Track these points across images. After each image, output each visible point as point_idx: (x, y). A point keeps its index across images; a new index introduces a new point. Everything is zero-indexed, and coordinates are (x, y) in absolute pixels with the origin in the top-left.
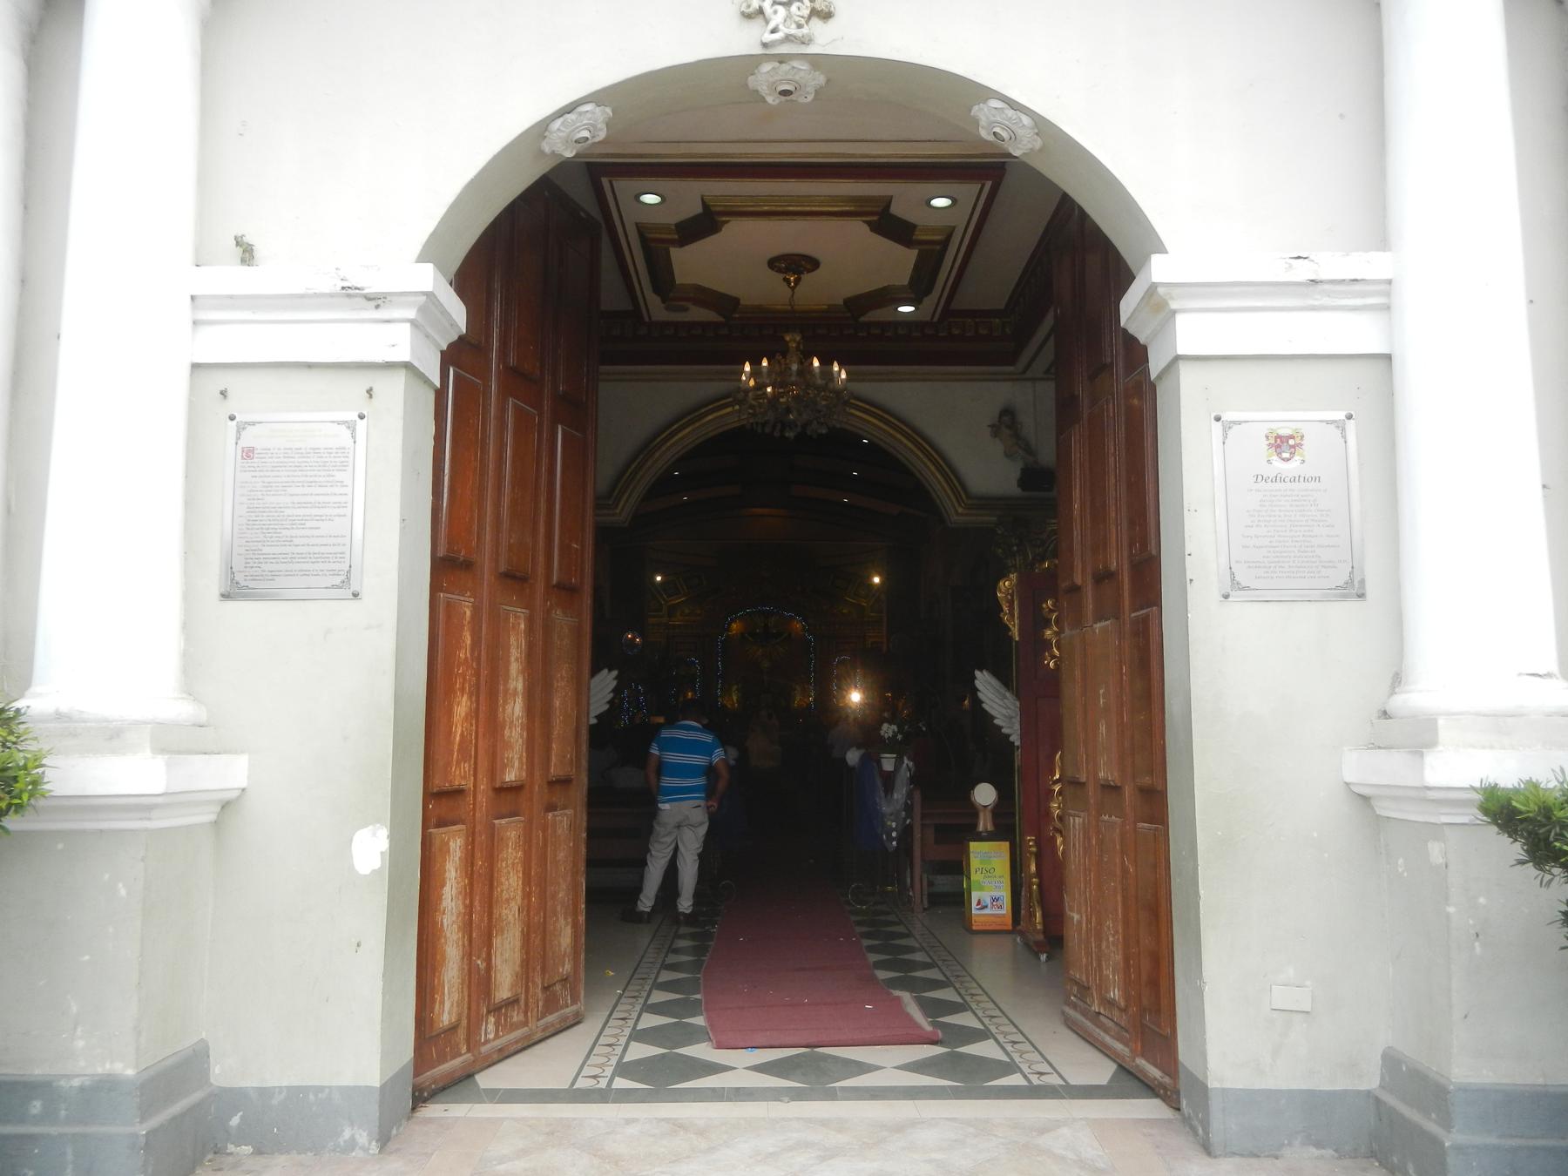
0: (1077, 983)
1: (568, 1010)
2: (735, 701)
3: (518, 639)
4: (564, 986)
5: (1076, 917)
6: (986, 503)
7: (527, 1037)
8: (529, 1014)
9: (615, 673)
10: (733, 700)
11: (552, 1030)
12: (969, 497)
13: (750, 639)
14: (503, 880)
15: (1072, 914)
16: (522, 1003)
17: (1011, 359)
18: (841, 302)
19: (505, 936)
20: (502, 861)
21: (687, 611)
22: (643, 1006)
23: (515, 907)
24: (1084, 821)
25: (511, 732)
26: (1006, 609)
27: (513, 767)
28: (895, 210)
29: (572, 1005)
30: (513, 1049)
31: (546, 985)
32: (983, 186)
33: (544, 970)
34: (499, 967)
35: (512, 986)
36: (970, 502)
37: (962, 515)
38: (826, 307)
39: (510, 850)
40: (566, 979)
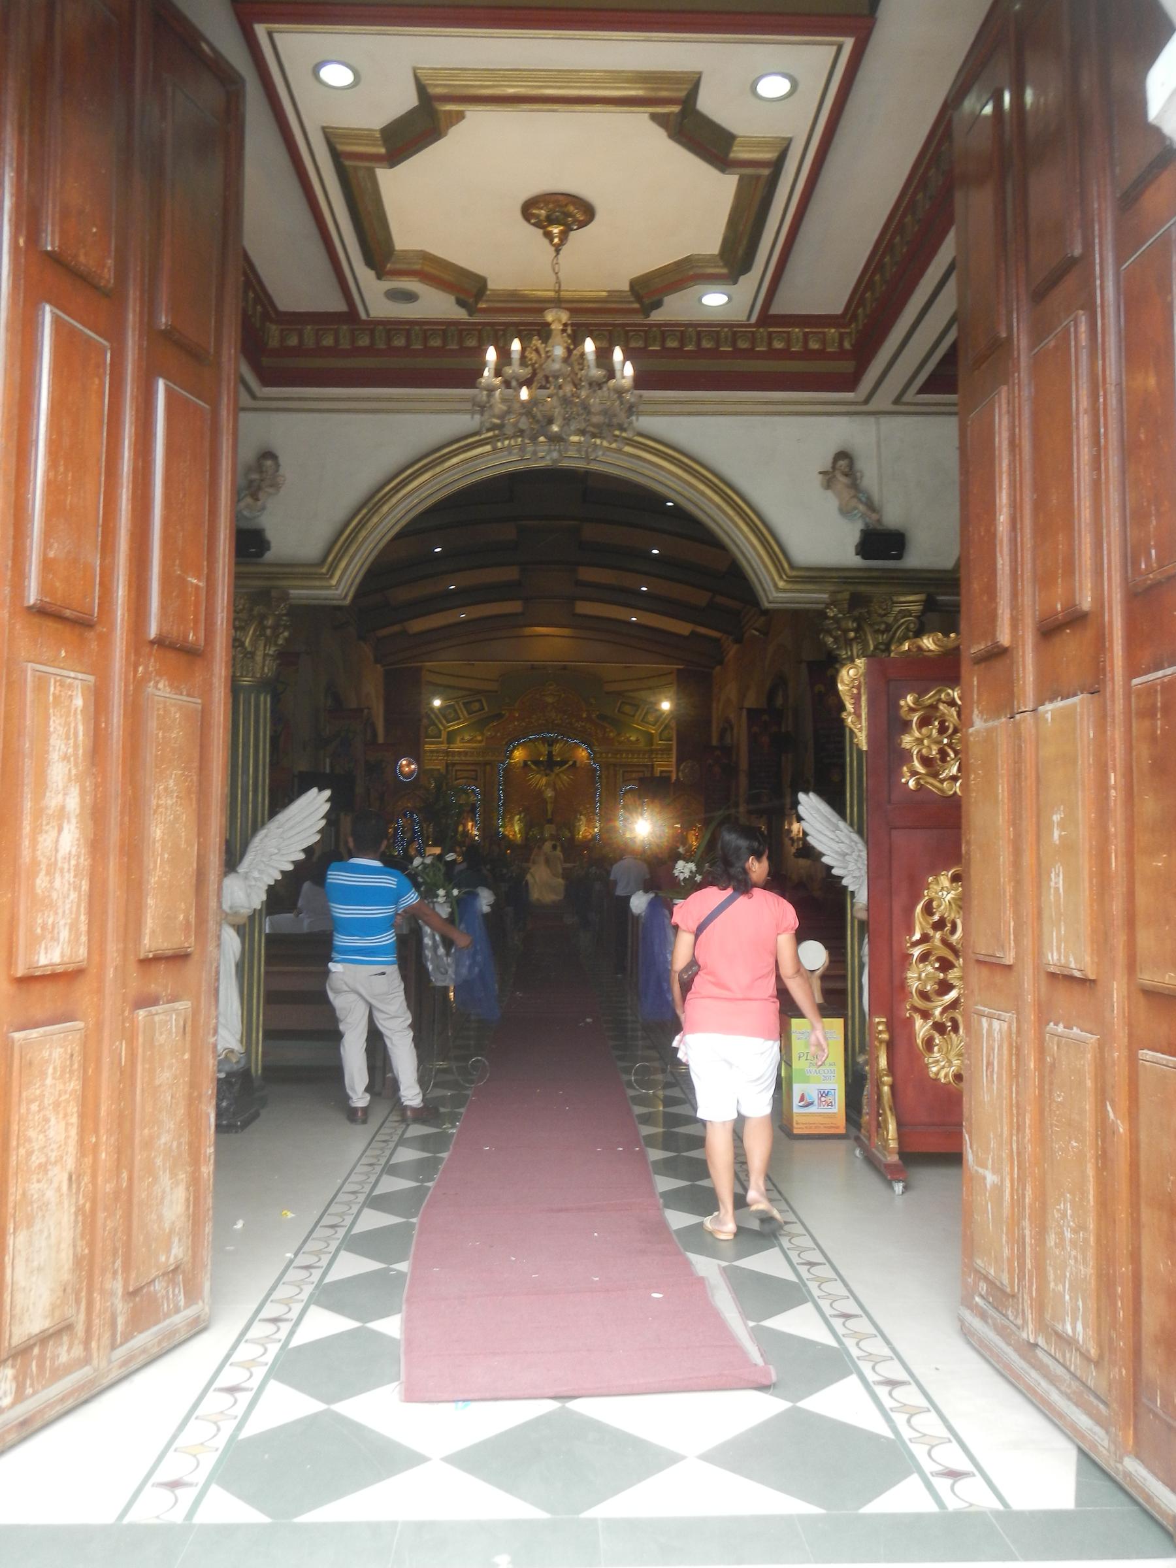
0: (986, 1278)
1: (177, 1319)
3: (67, 724)
4: (173, 1282)
5: (991, 1178)
6: (816, 576)
7: (92, 1382)
8: (94, 1344)
9: (327, 793)
11: (142, 1359)
12: (792, 566)
13: (533, 767)
14: (32, 1133)
15: (981, 1170)
16: (80, 1328)
17: (849, 382)
18: (626, 287)
19: (37, 1228)
20: (30, 1101)
21: (467, 738)
22: (317, 1287)
23: (59, 1176)
24: (1010, 1027)
25: (51, 882)
26: (850, 707)
27: (55, 939)
28: (707, 104)
29: (187, 1306)
30: (59, 1408)
31: (131, 1289)
32: (840, 48)
33: (127, 1266)
34: (23, 1284)
35: (54, 1307)
36: (794, 573)
37: (784, 591)
38: (604, 294)
39: (49, 1081)
40: (175, 1270)
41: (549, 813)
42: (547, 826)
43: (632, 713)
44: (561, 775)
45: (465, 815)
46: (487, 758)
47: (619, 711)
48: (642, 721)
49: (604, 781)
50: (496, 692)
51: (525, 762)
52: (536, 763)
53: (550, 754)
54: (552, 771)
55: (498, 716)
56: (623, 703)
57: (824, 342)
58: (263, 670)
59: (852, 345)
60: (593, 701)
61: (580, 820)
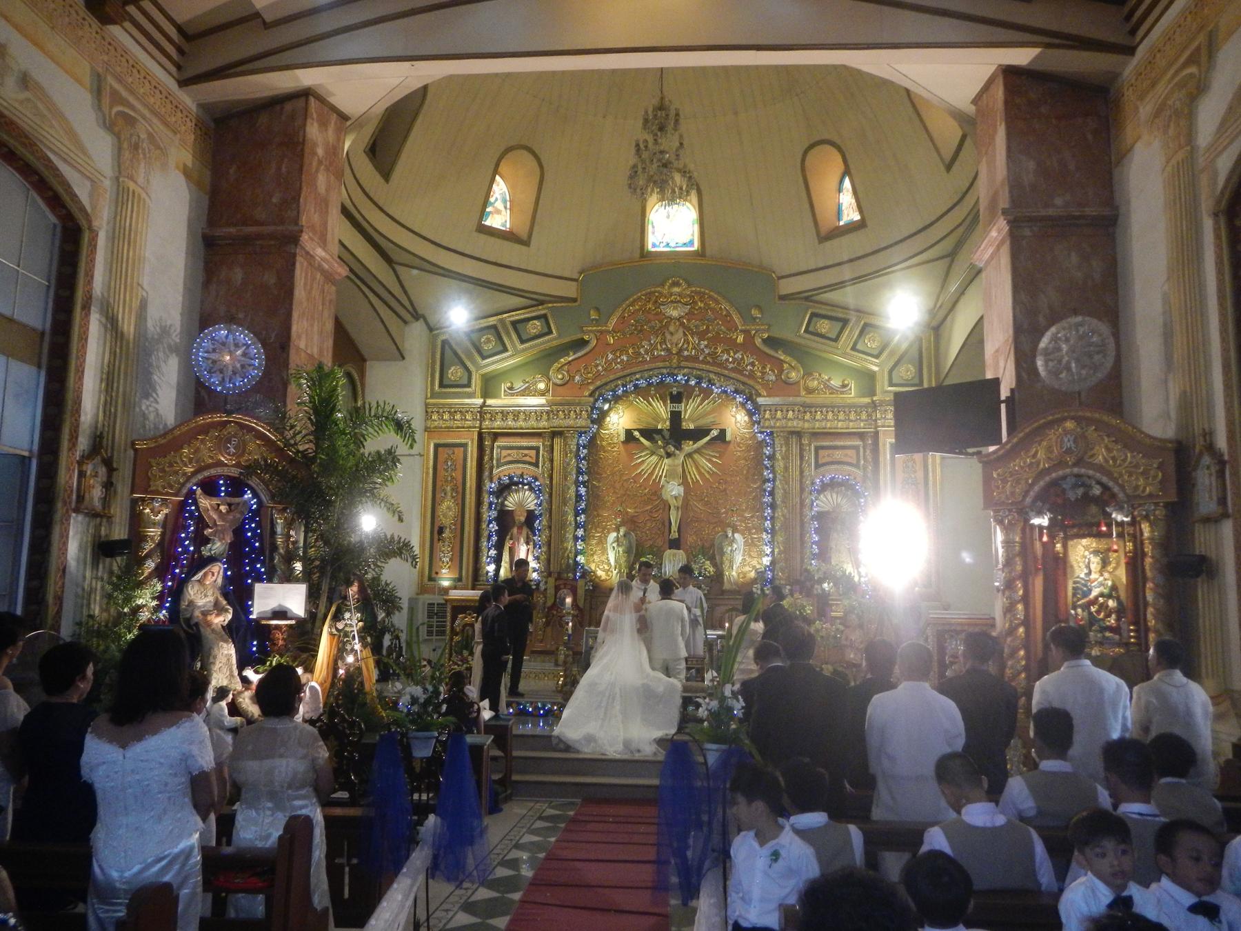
2: (613, 563)
10: (609, 564)
13: (642, 439)
21: (519, 385)
41: (674, 528)
42: (668, 552)
43: (833, 335)
44: (696, 456)
45: (515, 530)
46: (556, 422)
47: (806, 331)
48: (854, 348)
49: (780, 465)
50: (574, 300)
51: (629, 433)
53: (676, 417)
54: (679, 447)
55: (582, 343)
56: (813, 315)
60: (755, 312)
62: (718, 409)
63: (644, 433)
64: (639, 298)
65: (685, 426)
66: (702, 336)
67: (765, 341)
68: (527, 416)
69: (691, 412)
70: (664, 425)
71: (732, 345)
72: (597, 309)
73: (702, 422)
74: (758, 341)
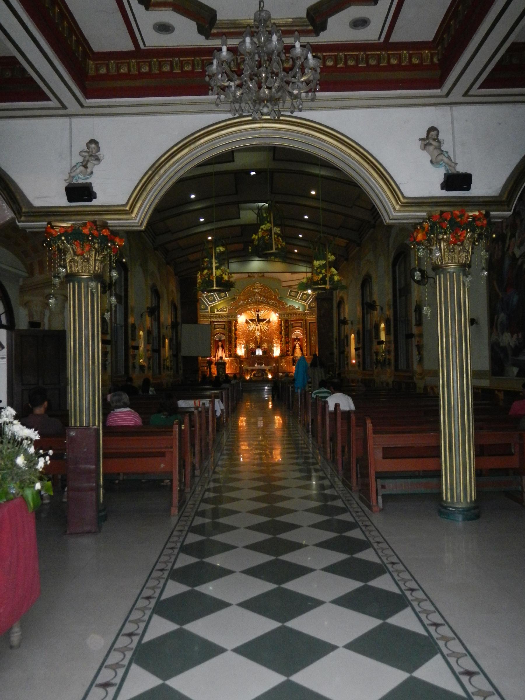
12: (404, 197)
17: (438, 83)
18: (304, 15)
36: (405, 201)
38: (291, 20)
41: (258, 343)
47: (289, 295)
48: (300, 299)
51: (246, 321)
52: (252, 320)
53: (258, 316)
56: (291, 291)
57: (421, 59)
58: (95, 267)
59: (438, 60)
61: (273, 346)
62: (268, 314)
63: (251, 320)
64: (248, 288)
65: (260, 318)
66: (264, 296)
67: (279, 298)
68: (222, 317)
69: (262, 314)
70: (255, 318)
71: (271, 299)
72: (238, 290)
73: (265, 318)
74: (278, 297)
